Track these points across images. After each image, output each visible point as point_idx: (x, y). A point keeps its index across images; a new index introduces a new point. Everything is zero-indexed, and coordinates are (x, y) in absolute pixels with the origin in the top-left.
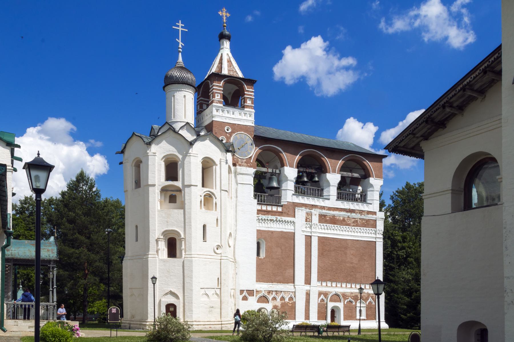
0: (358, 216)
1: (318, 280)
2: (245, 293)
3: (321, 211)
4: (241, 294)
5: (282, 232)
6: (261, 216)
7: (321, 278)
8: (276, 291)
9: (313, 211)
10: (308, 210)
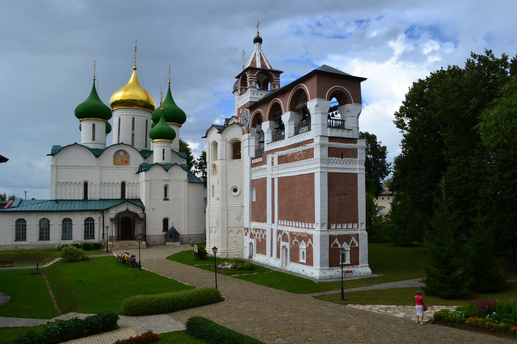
0: (300, 149)
1: (279, 219)
2: (246, 231)
5: (262, 178)
6: (253, 169)
7: (280, 218)
10: (272, 155)
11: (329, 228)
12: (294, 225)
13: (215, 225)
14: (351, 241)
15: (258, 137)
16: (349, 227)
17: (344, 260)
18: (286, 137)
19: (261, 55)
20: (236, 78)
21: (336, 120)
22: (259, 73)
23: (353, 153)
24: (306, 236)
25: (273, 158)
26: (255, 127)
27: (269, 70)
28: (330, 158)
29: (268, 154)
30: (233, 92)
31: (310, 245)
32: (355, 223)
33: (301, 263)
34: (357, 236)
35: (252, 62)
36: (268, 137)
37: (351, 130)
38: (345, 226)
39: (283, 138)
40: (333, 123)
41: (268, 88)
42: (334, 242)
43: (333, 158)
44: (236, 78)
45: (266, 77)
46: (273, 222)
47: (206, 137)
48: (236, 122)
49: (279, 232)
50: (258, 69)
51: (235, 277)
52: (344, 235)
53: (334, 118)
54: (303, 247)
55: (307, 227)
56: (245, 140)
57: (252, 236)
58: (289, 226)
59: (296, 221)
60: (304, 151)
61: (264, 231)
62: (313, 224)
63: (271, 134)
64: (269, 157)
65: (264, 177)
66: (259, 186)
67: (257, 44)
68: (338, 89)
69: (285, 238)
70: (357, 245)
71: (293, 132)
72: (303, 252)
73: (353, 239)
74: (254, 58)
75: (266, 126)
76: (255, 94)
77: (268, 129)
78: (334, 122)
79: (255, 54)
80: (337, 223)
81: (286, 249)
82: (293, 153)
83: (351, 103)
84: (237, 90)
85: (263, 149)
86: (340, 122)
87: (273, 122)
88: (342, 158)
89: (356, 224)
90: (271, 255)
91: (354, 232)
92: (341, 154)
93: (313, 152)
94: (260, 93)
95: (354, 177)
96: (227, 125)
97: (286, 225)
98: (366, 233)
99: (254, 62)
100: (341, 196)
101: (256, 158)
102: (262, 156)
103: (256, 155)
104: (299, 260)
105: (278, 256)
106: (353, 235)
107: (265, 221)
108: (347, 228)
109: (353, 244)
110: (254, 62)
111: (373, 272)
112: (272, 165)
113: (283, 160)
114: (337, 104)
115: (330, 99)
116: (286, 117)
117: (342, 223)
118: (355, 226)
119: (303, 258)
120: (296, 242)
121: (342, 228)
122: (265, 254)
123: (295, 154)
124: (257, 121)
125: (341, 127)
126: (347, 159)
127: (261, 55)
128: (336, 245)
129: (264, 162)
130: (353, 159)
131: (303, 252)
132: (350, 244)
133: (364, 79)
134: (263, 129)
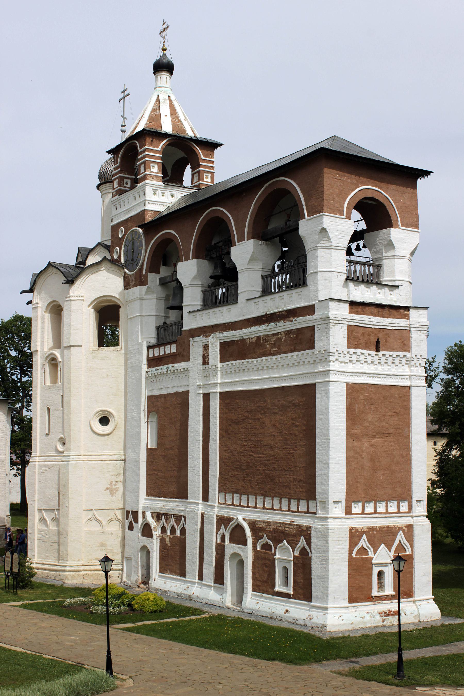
1: (220, 491)
3: (221, 335)
4: (127, 519)
8: (166, 514)
9: (210, 339)
11: (348, 511)
12: (259, 505)
13: (54, 504)
14: (397, 542)
15: (163, 296)
16: (390, 510)
17: (381, 586)
18: (242, 298)
19: (170, 101)
20: (109, 152)
21: (363, 264)
22: (169, 145)
23: (402, 341)
24: (293, 530)
25: (206, 348)
26: (158, 272)
27: (191, 139)
28: (352, 351)
29: (193, 336)
30: (98, 187)
31: (304, 552)
32: (404, 499)
33: (280, 594)
34: (409, 530)
35: (151, 119)
36: (192, 297)
37: (397, 287)
38: (381, 508)
39: (231, 298)
40: (355, 271)
41: (181, 181)
42: (360, 545)
43: (359, 351)
44: (109, 152)
45: (181, 154)
46: (205, 498)
47: (31, 291)
48: (109, 257)
49: (223, 521)
50: (166, 135)
51: (128, 630)
52: (381, 528)
53: (352, 258)
54: (284, 555)
55: (294, 508)
56: (131, 301)
57: (147, 531)
58: (248, 507)
59: (265, 496)
60: (288, 333)
61: (178, 518)
62: (311, 503)
63: (199, 289)
64: (196, 347)
65: (180, 390)
66: (169, 411)
67: (164, 75)
68: (369, 195)
69: (238, 536)
70: (408, 552)
71: (258, 286)
72: (286, 570)
73: (400, 537)
74: (156, 109)
75: (190, 272)
76: (159, 192)
77: (194, 278)
78: (353, 267)
79: (158, 100)
80: (366, 501)
81: (241, 563)
82: (259, 337)
83: (397, 227)
84: (112, 182)
85: (180, 323)
86: (371, 268)
87: (205, 263)
88: (377, 350)
89: (406, 503)
90: (200, 577)
91: (403, 522)
92: (376, 342)
93: (313, 336)
94: (168, 192)
95: (404, 393)
96: (84, 263)
97: (240, 506)
98: (427, 524)
99: (155, 117)
100: (374, 437)
101: (159, 344)
102: (175, 342)
103: (159, 337)
104: (274, 586)
105: (219, 578)
106: (400, 528)
107: (182, 493)
108: (387, 512)
109: (401, 547)
110: (155, 117)
111: (442, 615)
112: (205, 361)
113: (230, 351)
114: (363, 226)
115: (348, 217)
116: (245, 253)
117: (376, 500)
118: (404, 507)
119: (286, 583)
120: (266, 547)
121: (375, 512)
122: (183, 574)
123: (266, 338)
124: (165, 256)
125: (373, 279)
126: (388, 353)
127: (170, 101)
128: (363, 550)
129: (182, 355)
130: (402, 354)
131: (286, 570)
132: (394, 548)
133: (427, 173)
134: (180, 276)
